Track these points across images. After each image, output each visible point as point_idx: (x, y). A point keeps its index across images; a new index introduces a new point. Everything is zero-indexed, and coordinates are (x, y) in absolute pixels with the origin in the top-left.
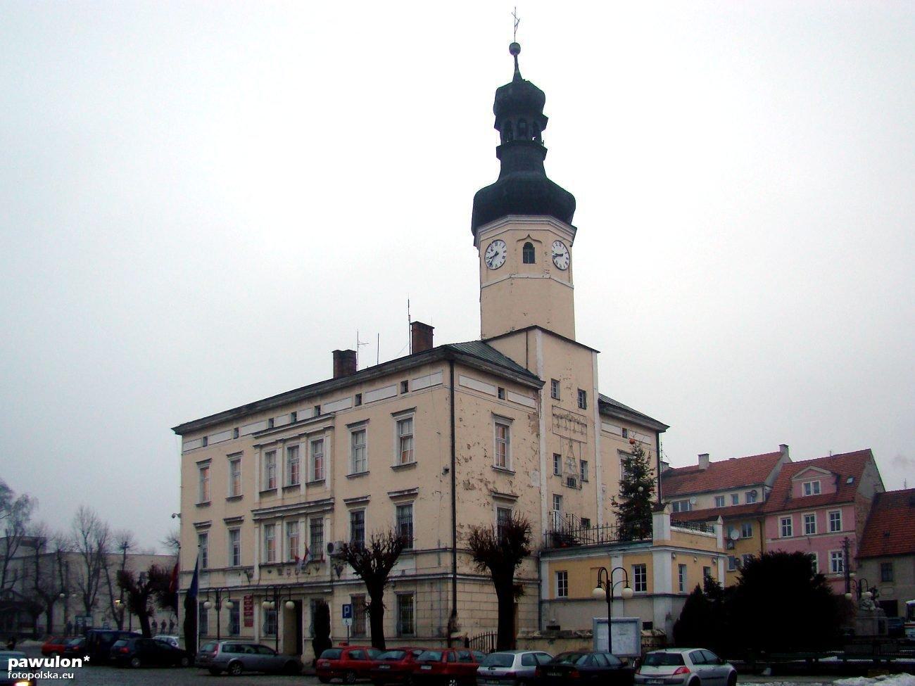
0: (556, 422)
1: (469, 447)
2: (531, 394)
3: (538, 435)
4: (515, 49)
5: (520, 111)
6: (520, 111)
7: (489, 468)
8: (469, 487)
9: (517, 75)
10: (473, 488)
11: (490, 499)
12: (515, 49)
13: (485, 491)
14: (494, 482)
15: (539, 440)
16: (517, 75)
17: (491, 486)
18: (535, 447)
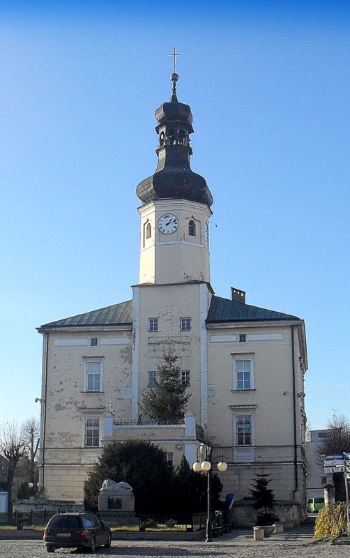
0: (152, 348)
1: (61, 383)
2: (125, 335)
3: (131, 362)
4: (175, 77)
5: (176, 120)
6: (176, 120)
7: (80, 394)
8: (58, 408)
9: (174, 97)
10: (64, 408)
11: (79, 414)
12: (175, 77)
13: (74, 408)
14: (83, 402)
15: (131, 366)
16: (174, 97)
17: (80, 405)
18: (127, 371)
